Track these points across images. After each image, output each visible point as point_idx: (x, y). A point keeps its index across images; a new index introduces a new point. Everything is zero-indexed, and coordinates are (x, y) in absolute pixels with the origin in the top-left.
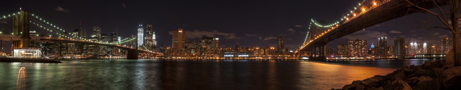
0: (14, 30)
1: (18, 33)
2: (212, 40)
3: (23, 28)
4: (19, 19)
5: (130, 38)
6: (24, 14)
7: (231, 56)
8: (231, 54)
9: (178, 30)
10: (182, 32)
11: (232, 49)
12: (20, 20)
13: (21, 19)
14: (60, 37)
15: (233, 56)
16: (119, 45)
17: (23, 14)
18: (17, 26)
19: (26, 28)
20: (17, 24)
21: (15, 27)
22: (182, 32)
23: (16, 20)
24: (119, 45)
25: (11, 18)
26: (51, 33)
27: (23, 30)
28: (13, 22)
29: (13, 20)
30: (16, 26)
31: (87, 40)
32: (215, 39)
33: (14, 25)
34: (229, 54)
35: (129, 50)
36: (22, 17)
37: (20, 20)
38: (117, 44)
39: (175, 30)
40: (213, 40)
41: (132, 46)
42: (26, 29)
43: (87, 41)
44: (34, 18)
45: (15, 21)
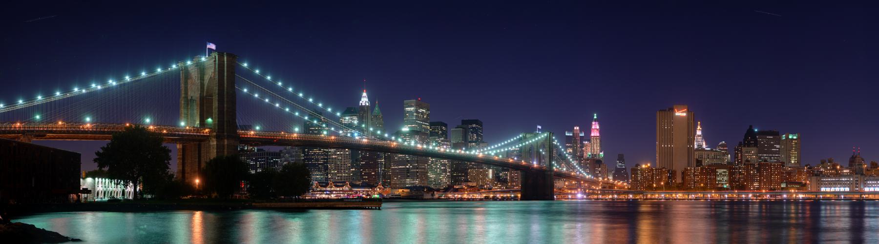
0: (183, 111)
1: (198, 122)
2: (779, 141)
3: (215, 104)
4: (202, 79)
5: (528, 136)
6: (217, 62)
7: (842, 189)
8: (844, 185)
9: (672, 110)
10: (684, 114)
11: (841, 167)
12: (203, 80)
13: (207, 78)
14: (325, 133)
15: (847, 189)
16: (498, 156)
17: (215, 61)
18: (193, 98)
19: (225, 105)
20: (194, 93)
21: (189, 102)
22: (684, 114)
23: (189, 81)
24: (498, 156)
25: (176, 75)
26: (298, 121)
27: (215, 111)
28: (182, 85)
29: (182, 81)
30: (189, 98)
31: (406, 143)
32: (787, 138)
33: (183, 95)
34: (835, 184)
35: (527, 171)
36: (210, 73)
37: (206, 82)
38: (493, 154)
39: (665, 110)
40: (780, 138)
41: (535, 160)
42: (225, 110)
43: (406, 146)
44: (249, 74)
45: (186, 83)
